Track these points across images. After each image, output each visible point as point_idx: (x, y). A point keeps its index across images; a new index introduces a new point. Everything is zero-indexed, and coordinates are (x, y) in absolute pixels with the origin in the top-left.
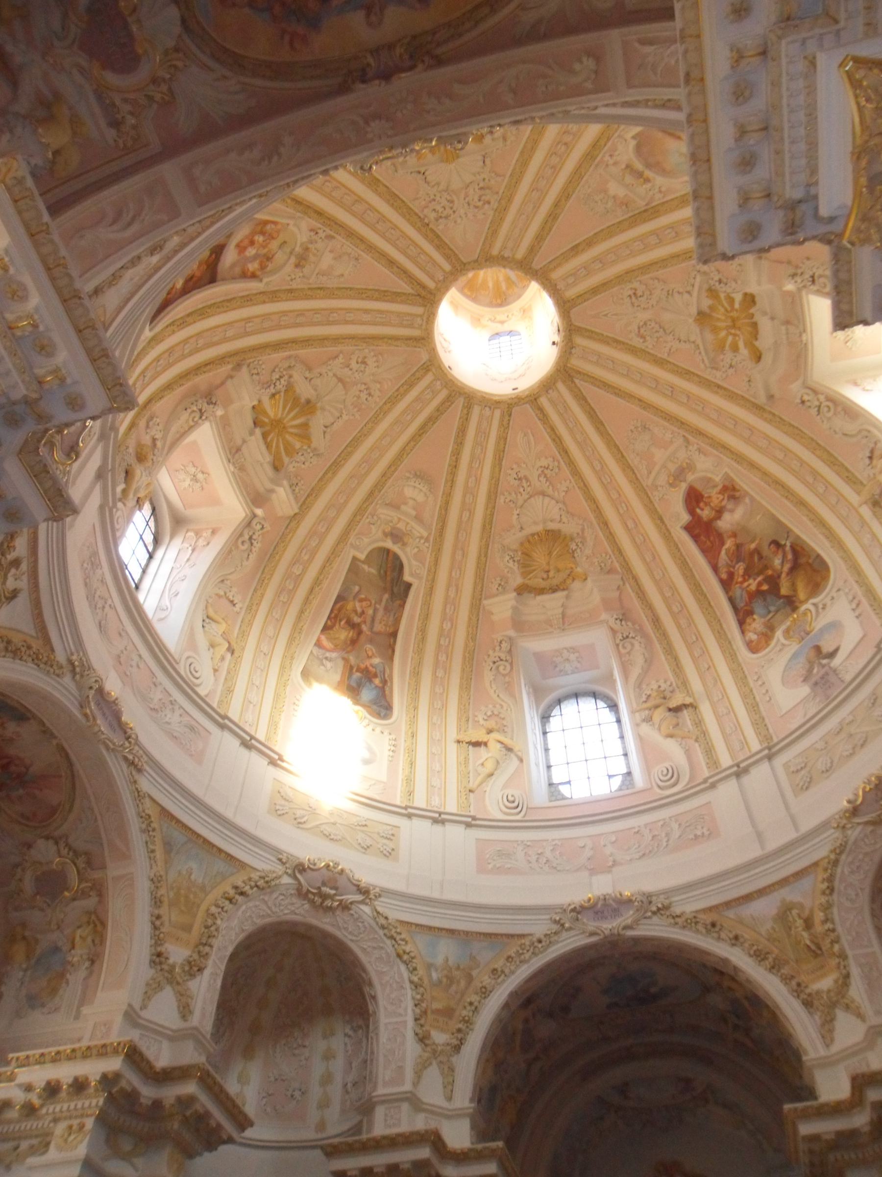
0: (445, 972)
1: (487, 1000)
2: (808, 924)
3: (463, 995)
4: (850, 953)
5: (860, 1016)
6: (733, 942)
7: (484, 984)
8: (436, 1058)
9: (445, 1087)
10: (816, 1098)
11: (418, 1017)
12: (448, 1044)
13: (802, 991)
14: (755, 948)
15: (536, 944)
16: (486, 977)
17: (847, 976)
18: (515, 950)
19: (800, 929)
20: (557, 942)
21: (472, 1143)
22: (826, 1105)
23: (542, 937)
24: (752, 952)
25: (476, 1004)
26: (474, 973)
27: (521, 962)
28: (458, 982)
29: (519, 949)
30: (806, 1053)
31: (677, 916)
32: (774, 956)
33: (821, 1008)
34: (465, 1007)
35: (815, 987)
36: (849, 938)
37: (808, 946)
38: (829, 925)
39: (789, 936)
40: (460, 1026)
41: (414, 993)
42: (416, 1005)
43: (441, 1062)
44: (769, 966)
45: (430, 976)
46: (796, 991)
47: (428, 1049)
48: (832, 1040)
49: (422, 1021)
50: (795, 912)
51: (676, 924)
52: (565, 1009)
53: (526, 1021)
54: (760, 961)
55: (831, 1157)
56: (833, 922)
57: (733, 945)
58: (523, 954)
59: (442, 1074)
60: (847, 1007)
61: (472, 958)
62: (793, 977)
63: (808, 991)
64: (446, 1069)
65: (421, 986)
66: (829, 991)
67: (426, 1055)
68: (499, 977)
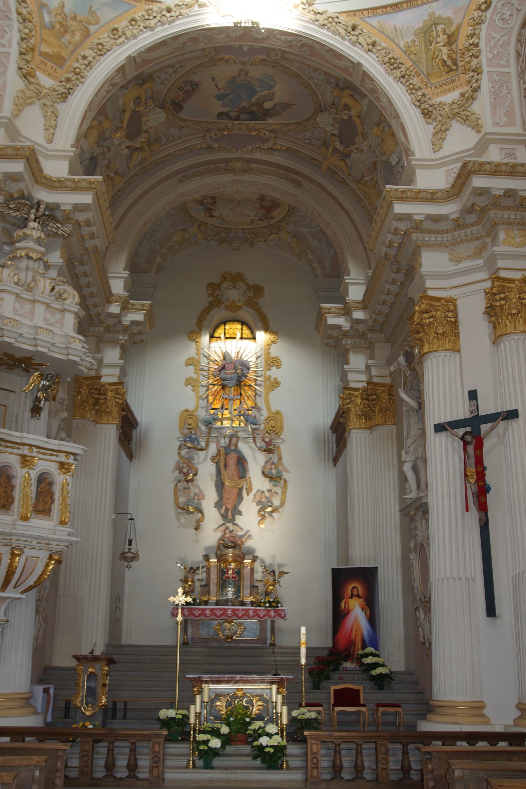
0: (59, 18)
1: (103, 58)
2: (451, 39)
3: (76, 47)
4: (485, 69)
5: (477, 127)
6: (370, 47)
7: (101, 41)
8: (39, 99)
9: (46, 129)
10: (416, 186)
11: (24, 51)
12: (54, 90)
13: (425, 102)
14: (391, 56)
15: (164, 12)
16: (106, 35)
17: (475, 90)
18: (140, 14)
19: (442, 44)
20: (189, 16)
21: (70, 172)
22: (426, 191)
23: (172, 6)
24: (386, 60)
25: (90, 58)
26: (92, 28)
27: (145, 28)
28: (73, 33)
29: (145, 13)
30: (413, 154)
31: (318, 13)
32: (407, 66)
33: (440, 118)
34: (78, 61)
35: (439, 100)
36: (490, 56)
37: (445, 62)
38: (475, 40)
39: (428, 50)
40: (70, 76)
41: (21, 26)
42: (22, 39)
43: (44, 104)
44: (399, 75)
45: (41, 17)
46: (419, 101)
47: (32, 87)
48: (441, 148)
49: (28, 58)
50: (440, 27)
51: (317, 21)
52: (178, 106)
53: (137, 100)
54: (391, 70)
55: (414, 236)
56: (479, 38)
57: (369, 50)
58: (148, 19)
59: (45, 116)
60: (466, 120)
61: (92, 12)
62: (421, 88)
63: (430, 102)
64: (49, 111)
65: (31, 22)
66: (453, 103)
67: (29, 93)
68: (120, 37)
